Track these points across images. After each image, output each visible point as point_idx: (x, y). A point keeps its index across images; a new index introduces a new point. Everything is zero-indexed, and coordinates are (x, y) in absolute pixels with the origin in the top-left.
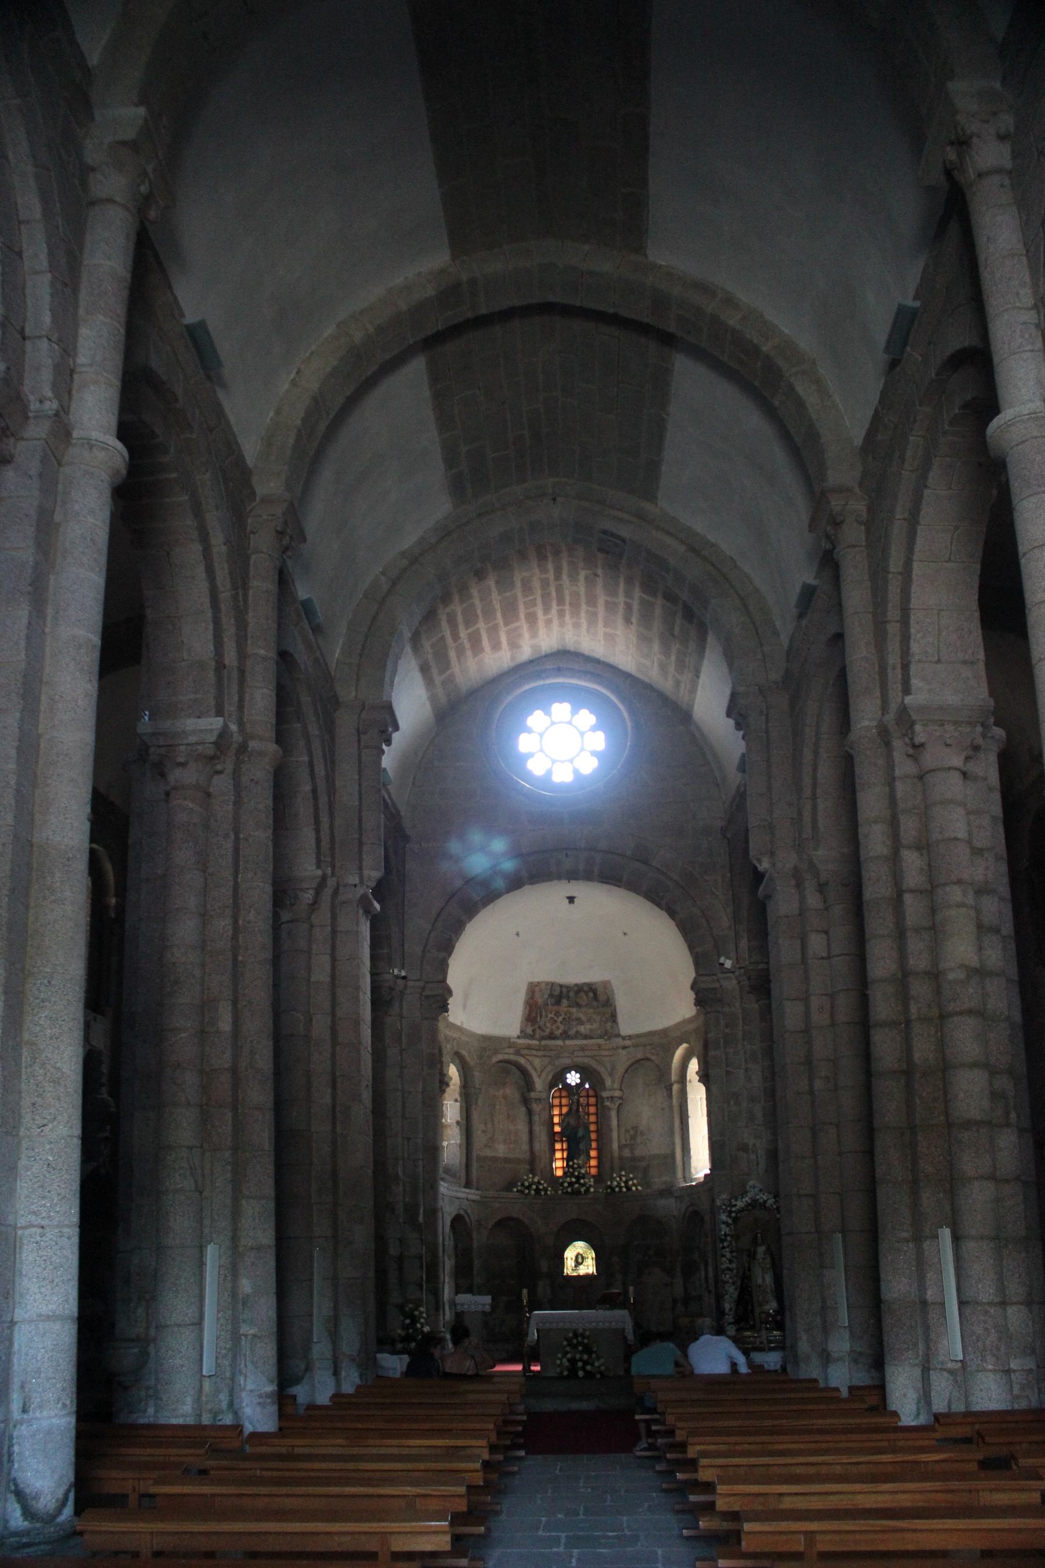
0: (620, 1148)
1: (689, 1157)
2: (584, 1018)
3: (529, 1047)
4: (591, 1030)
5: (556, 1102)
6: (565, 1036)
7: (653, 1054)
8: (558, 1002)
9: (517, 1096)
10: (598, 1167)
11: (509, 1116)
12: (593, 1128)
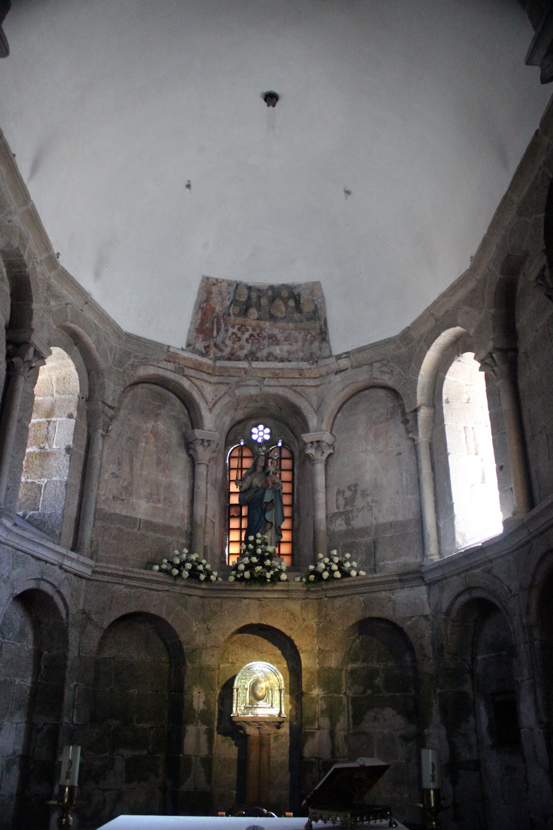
0: (330, 518)
1: (451, 516)
2: (280, 336)
3: (198, 367)
4: (289, 353)
5: (234, 463)
6: (252, 356)
7: (383, 372)
8: (245, 312)
9: (175, 438)
10: (292, 555)
11: (159, 462)
12: (286, 488)
